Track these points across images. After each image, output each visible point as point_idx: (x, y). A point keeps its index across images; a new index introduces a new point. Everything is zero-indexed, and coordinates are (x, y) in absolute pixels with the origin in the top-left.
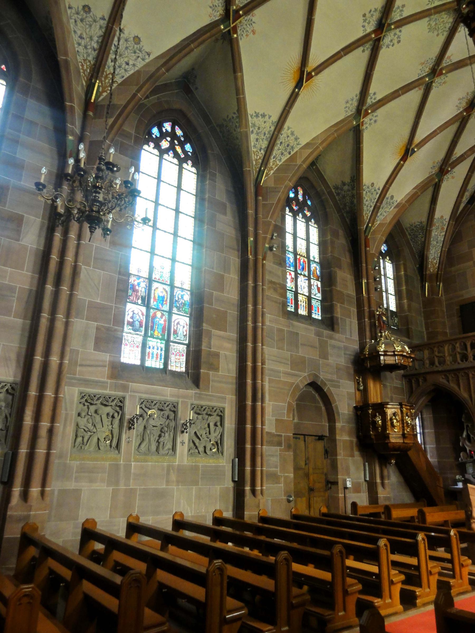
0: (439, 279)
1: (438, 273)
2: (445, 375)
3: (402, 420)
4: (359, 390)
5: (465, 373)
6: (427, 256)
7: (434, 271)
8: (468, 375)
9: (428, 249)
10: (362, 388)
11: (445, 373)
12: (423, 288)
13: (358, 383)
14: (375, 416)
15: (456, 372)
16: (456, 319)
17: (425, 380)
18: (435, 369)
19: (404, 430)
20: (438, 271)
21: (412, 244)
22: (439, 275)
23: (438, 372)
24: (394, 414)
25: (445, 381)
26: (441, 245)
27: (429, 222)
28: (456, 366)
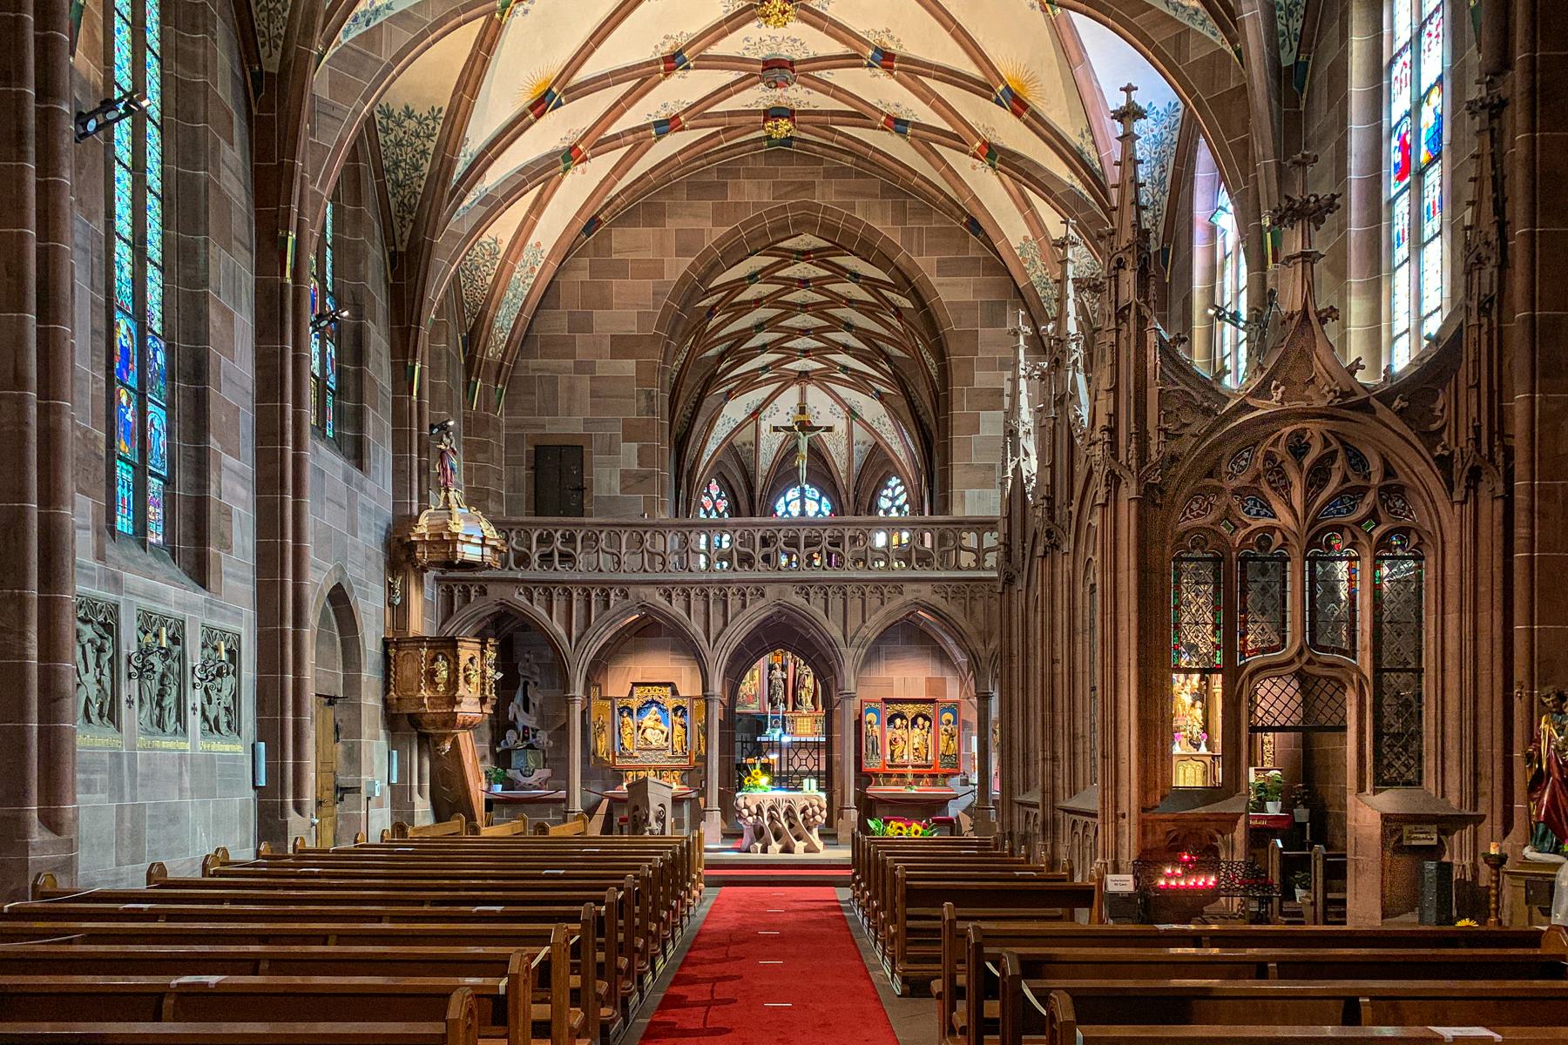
0: (501, 379)
1: (501, 365)
2: (526, 589)
3: (484, 672)
4: (391, 604)
5: (565, 590)
6: (492, 320)
7: (495, 355)
8: (571, 594)
9: (497, 308)
10: (398, 601)
11: (528, 586)
12: (469, 387)
13: (391, 589)
14: (435, 660)
15: (548, 586)
16: (523, 473)
17: (483, 592)
18: (511, 575)
19: (484, 690)
20: (503, 359)
21: (462, 279)
22: (504, 371)
23: (516, 581)
24: (471, 660)
25: (523, 599)
26: (520, 305)
27: (515, 250)
28: (550, 575)
